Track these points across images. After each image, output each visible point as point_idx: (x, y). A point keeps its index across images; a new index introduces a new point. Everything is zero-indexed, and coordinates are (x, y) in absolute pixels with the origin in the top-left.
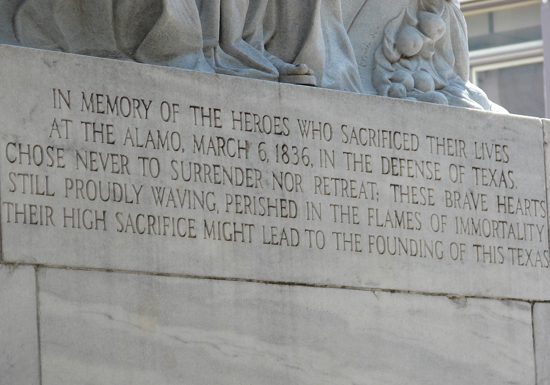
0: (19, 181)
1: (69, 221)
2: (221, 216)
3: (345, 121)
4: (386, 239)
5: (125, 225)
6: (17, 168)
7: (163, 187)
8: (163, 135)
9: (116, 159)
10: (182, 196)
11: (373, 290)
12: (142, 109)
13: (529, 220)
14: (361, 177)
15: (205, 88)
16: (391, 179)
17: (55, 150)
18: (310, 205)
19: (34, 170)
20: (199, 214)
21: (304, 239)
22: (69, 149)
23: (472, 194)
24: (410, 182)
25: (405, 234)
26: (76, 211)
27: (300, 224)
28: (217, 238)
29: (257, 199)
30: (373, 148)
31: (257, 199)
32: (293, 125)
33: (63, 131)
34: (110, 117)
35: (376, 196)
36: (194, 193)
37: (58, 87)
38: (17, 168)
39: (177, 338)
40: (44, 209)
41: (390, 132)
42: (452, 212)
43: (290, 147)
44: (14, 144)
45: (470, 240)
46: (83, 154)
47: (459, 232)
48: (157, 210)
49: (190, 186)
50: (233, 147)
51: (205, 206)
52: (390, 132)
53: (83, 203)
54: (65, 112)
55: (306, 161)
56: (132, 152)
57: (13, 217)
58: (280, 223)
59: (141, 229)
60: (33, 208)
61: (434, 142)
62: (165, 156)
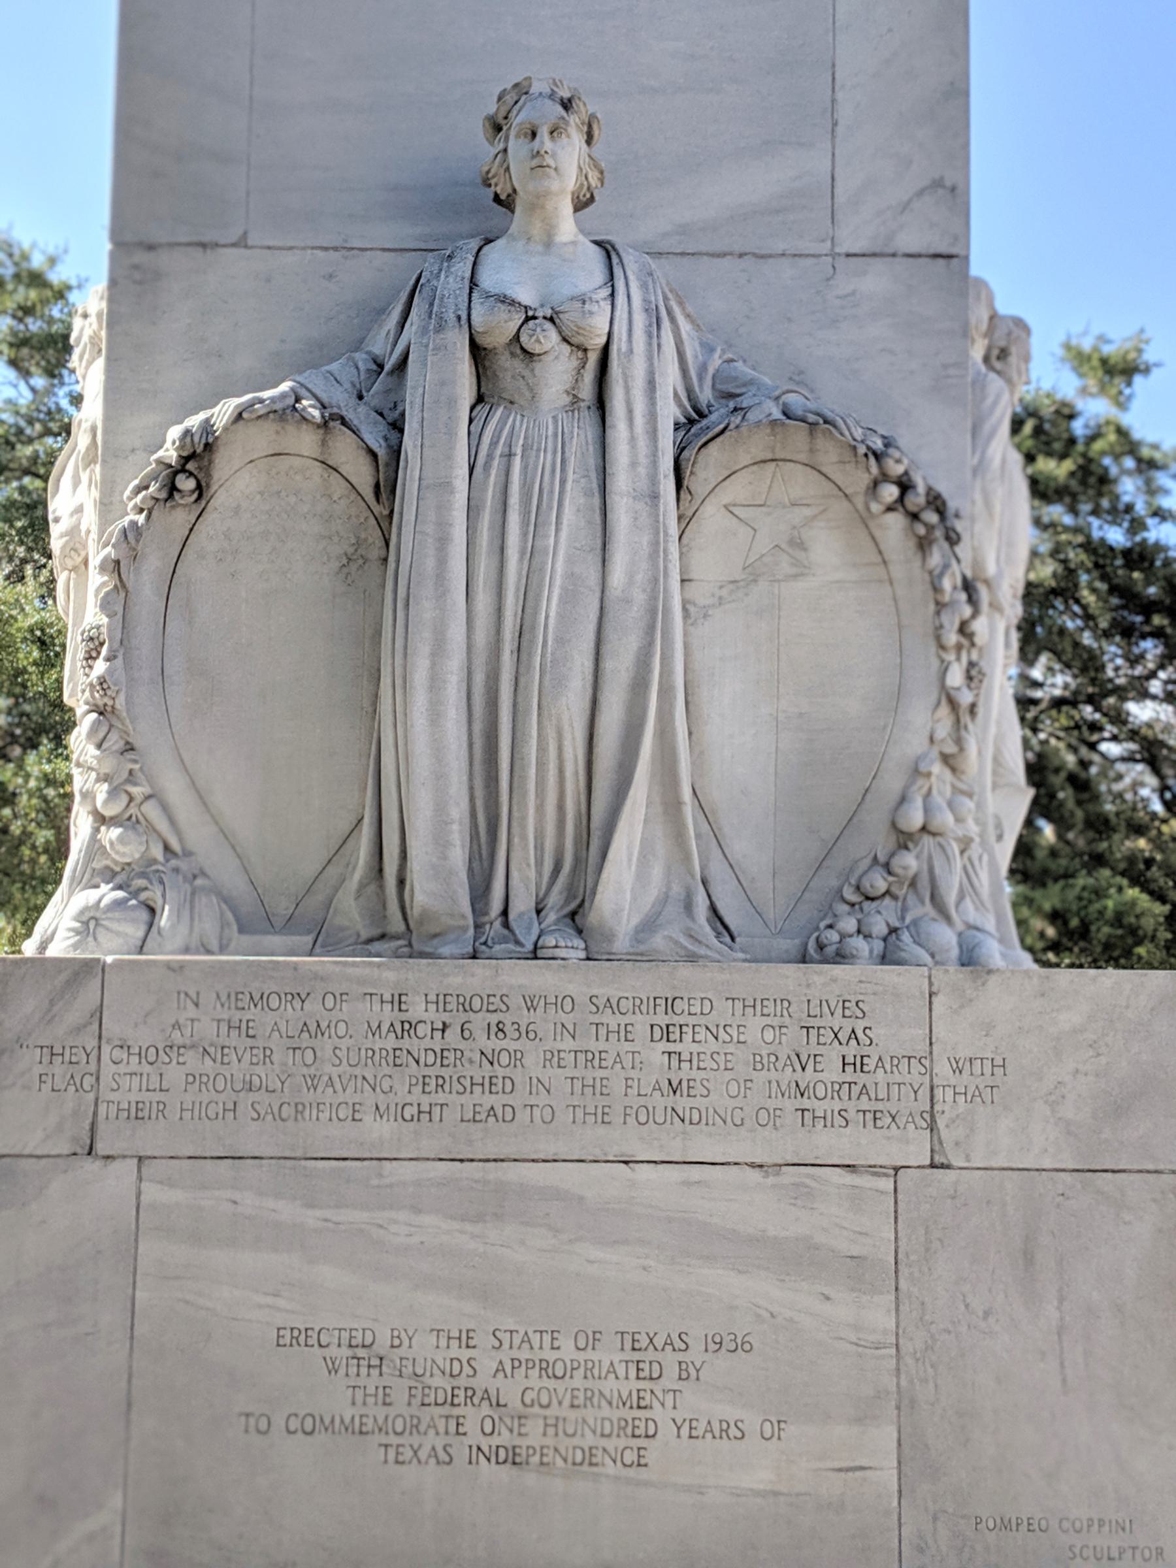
0: (125, 1082)
1: (187, 1115)
2: (402, 1095)
3: (595, 992)
4: (651, 1109)
5: (262, 1113)
6: (122, 1069)
7: (318, 1074)
8: (324, 1025)
9: (255, 1051)
10: (345, 1082)
11: (626, 1162)
12: (297, 1004)
13: (897, 1078)
14: (613, 1046)
15: (390, 975)
16: (663, 1046)
17: (175, 1049)
18: (535, 1081)
19: (147, 1068)
20: (369, 1098)
21: (523, 1116)
22: (193, 1046)
23: (798, 1056)
24: (695, 1048)
25: (682, 1103)
26: (197, 1105)
27: (516, 1100)
28: (392, 1119)
29: (455, 1078)
30: (639, 1016)
31: (455, 1078)
32: (516, 1001)
33: (188, 1032)
34: (252, 1013)
35: (638, 1066)
36: (364, 1078)
37: (183, 988)
38: (122, 1069)
39: (326, 1220)
40: (155, 1105)
41: (667, 999)
42: (761, 1077)
43: (508, 1023)
44: (122, 1047)
45: (789, 1105)
46: (212, 1050)
47: (773, 1095)
48: (308, 1097)
49: (358, 1071)
50: (422, 1030)
51: (378, 1089)
52: (667, 999)
53: (205, 1097)
54: (192, 1012)
55: (532, 1035)
56: (275, 1042)
57: (112, 1115)
58: (488, 1100)
59: (284, 1115)
60: (140, 1106)
61: (739, 1005)
62: (326, 1046)
